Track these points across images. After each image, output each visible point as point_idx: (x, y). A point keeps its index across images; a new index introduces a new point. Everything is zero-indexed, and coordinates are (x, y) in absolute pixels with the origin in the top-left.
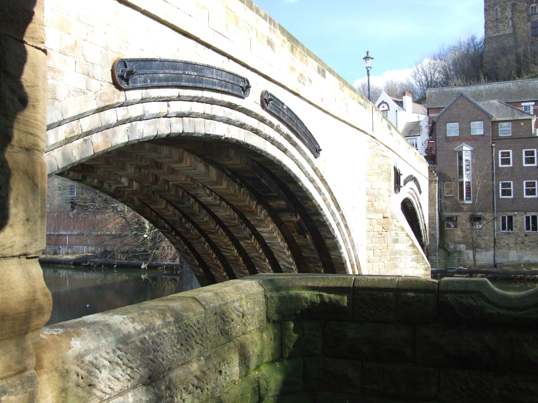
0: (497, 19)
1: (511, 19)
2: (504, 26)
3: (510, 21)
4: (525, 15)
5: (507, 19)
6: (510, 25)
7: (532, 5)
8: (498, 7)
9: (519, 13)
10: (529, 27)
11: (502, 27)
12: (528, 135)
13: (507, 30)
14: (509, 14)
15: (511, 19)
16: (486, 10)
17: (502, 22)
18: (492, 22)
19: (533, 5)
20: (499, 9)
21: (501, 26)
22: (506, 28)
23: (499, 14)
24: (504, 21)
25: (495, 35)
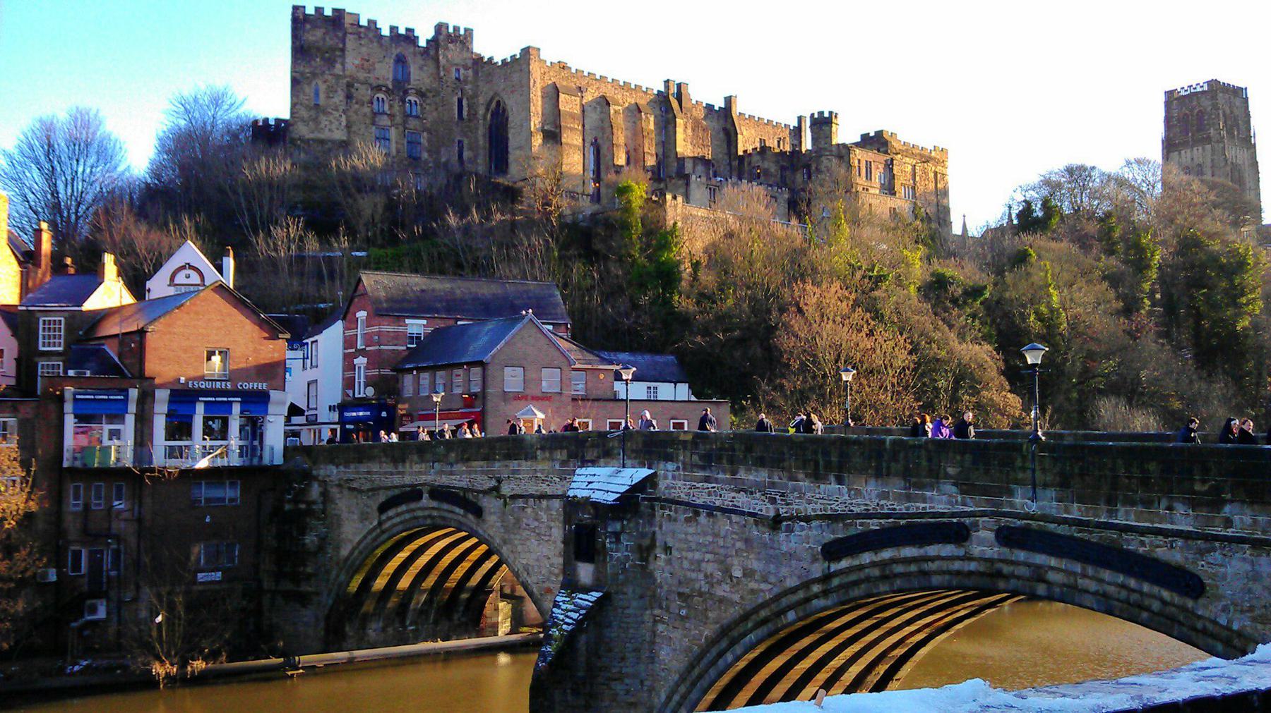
0: (317, 105)
1: (344, 112)
2: (331, 122)
3: (343, 116)
4: (367, 110)
5: (337, 110)
6: (344, 123)
7: (378, 95)
8: (320, 83)
9: (357, 103)
10: (373, 135)
11: (327, 123)
12: (609, 395)
13: (336, 131)
14: (339, 98)
15: (344, 112)
16: (295, 82)
17: (325, 113)
18: (308, 108)
19: (381, 96)
20: (323, 87)
21: (324, 120)
22: (334, 127)
23: (322, 96)
24: (331, 114)
25: (312, 136)
